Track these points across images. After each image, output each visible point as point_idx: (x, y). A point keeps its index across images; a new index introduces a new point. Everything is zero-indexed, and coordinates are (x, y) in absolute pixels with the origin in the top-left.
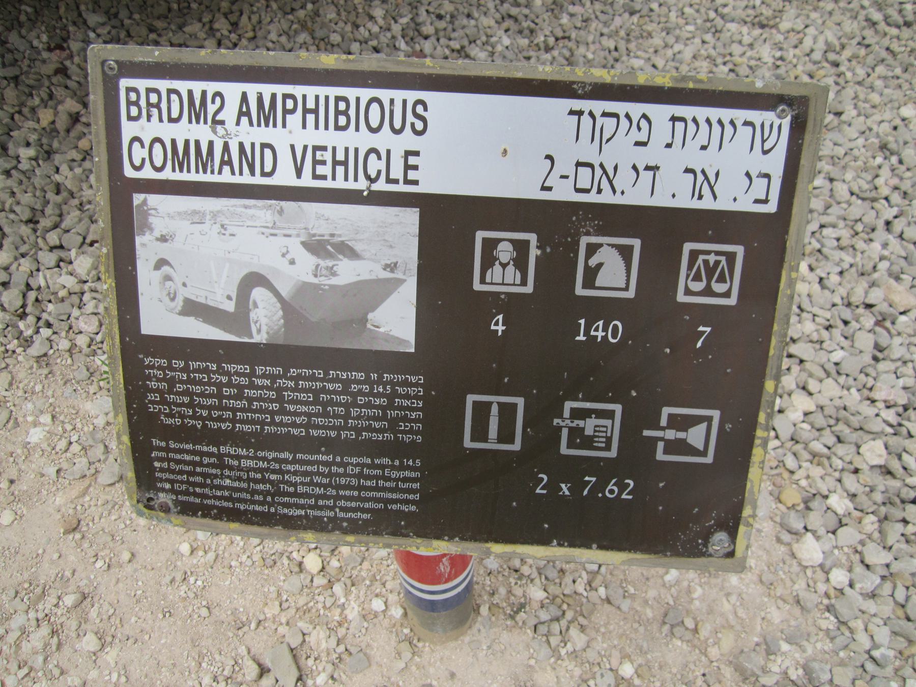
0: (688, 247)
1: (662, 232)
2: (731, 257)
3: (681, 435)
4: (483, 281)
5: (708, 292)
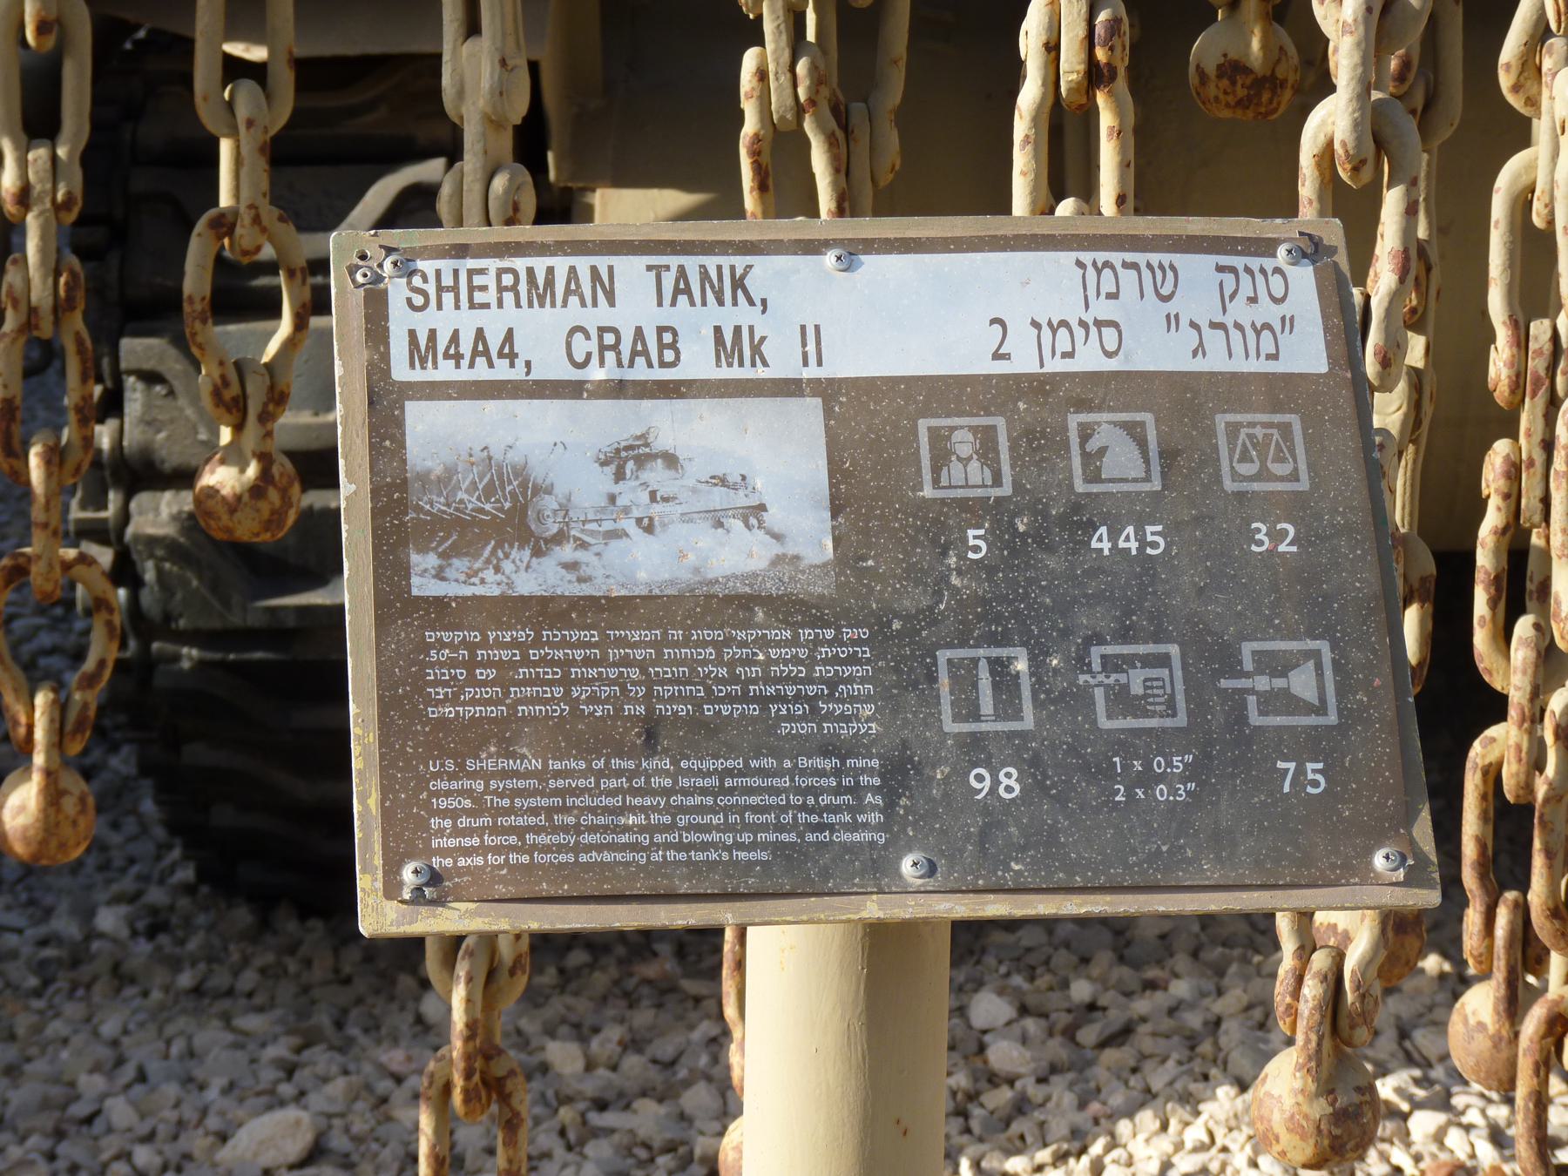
2: (1285, 429)
3: (1279, 683)
4: (936, 482)
5: (1263, 475)
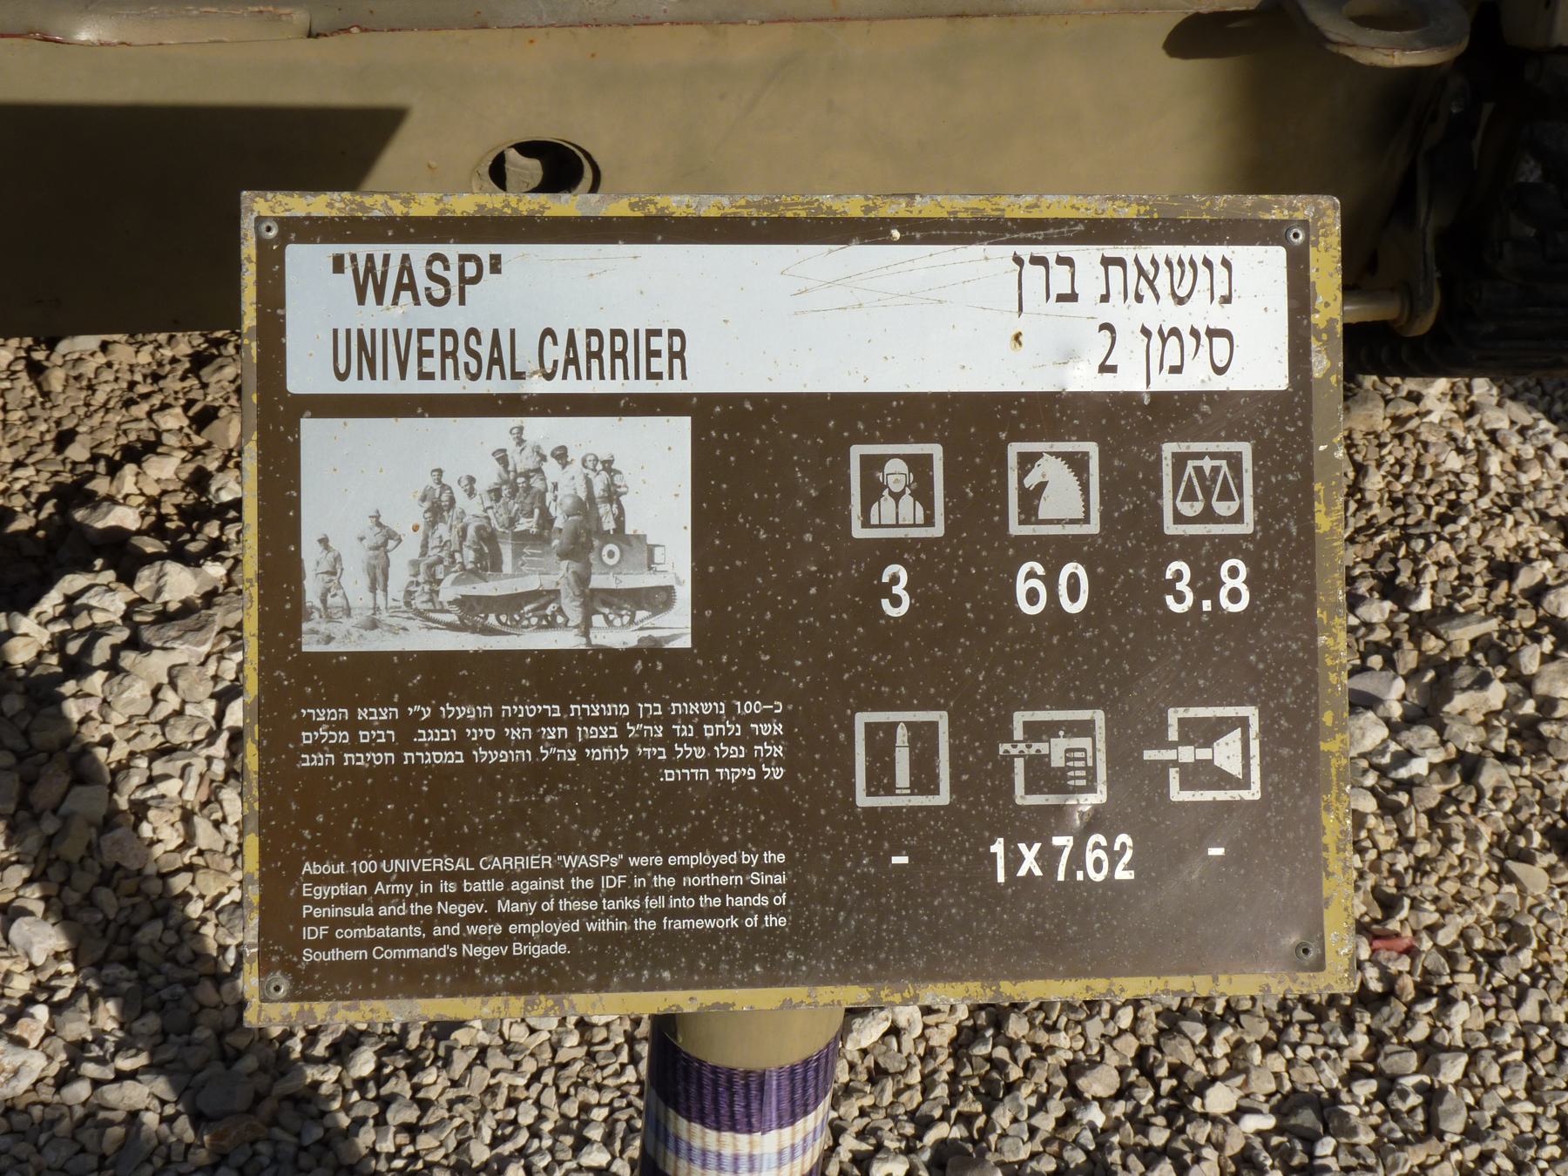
0: (1169, 449)
1: (1128, 430)
2: (1234, 460)
3: (1204, 754)
4: (866, 523)
5: (1208, 516)
